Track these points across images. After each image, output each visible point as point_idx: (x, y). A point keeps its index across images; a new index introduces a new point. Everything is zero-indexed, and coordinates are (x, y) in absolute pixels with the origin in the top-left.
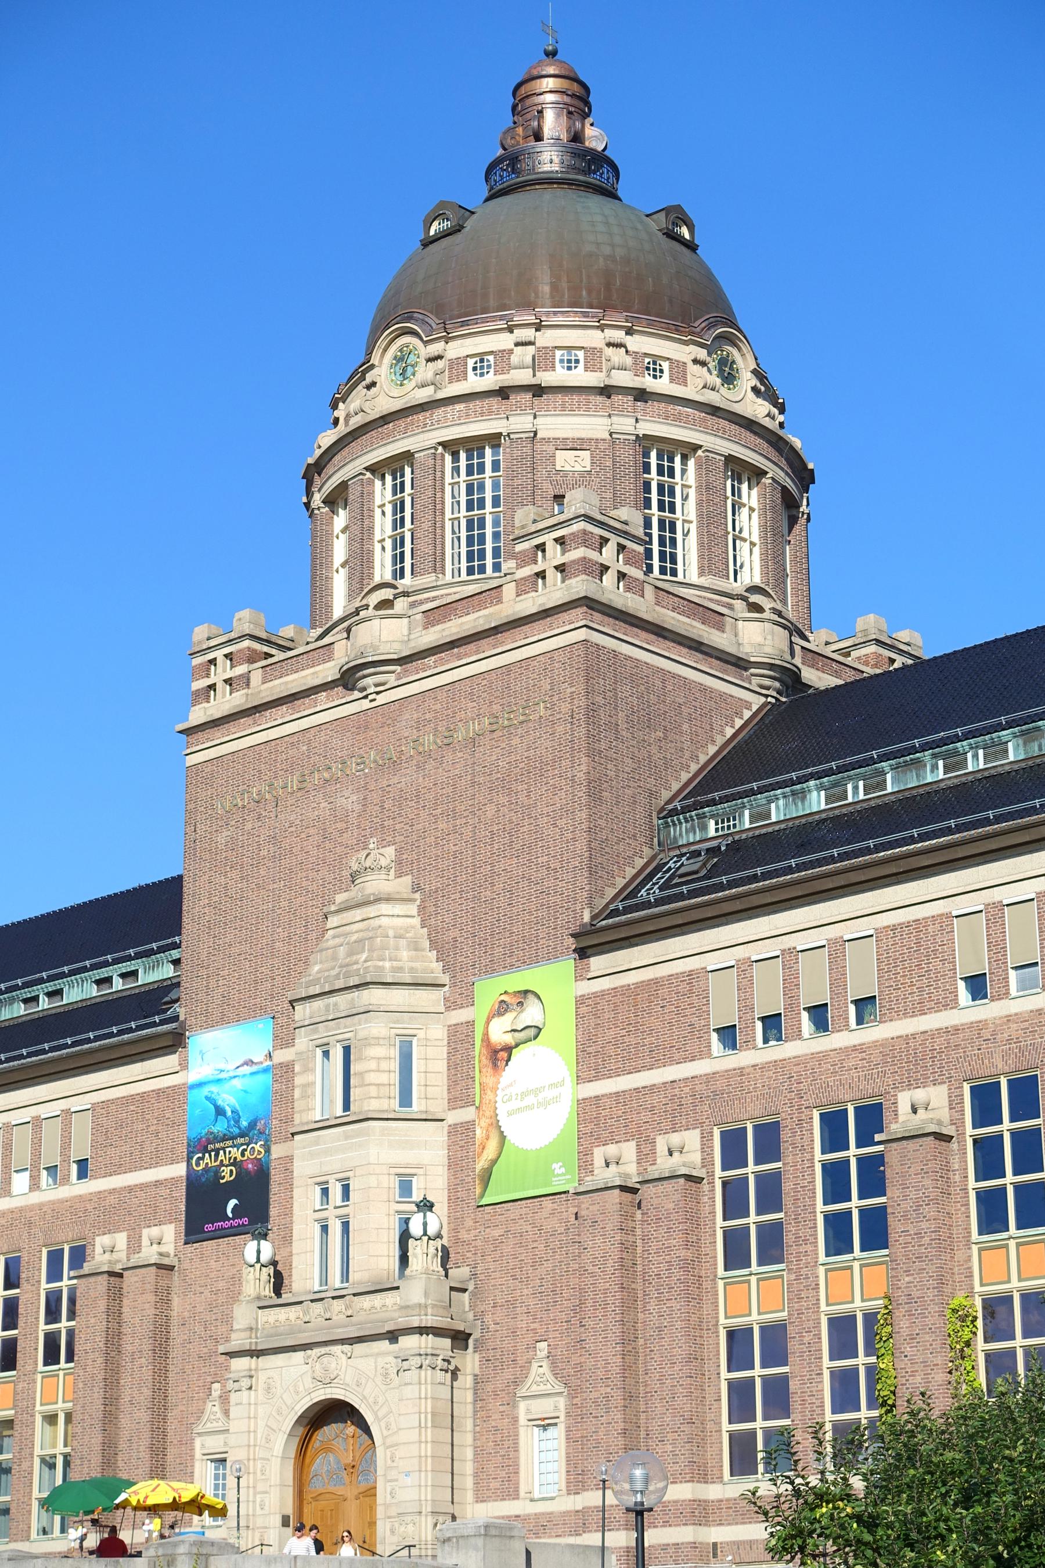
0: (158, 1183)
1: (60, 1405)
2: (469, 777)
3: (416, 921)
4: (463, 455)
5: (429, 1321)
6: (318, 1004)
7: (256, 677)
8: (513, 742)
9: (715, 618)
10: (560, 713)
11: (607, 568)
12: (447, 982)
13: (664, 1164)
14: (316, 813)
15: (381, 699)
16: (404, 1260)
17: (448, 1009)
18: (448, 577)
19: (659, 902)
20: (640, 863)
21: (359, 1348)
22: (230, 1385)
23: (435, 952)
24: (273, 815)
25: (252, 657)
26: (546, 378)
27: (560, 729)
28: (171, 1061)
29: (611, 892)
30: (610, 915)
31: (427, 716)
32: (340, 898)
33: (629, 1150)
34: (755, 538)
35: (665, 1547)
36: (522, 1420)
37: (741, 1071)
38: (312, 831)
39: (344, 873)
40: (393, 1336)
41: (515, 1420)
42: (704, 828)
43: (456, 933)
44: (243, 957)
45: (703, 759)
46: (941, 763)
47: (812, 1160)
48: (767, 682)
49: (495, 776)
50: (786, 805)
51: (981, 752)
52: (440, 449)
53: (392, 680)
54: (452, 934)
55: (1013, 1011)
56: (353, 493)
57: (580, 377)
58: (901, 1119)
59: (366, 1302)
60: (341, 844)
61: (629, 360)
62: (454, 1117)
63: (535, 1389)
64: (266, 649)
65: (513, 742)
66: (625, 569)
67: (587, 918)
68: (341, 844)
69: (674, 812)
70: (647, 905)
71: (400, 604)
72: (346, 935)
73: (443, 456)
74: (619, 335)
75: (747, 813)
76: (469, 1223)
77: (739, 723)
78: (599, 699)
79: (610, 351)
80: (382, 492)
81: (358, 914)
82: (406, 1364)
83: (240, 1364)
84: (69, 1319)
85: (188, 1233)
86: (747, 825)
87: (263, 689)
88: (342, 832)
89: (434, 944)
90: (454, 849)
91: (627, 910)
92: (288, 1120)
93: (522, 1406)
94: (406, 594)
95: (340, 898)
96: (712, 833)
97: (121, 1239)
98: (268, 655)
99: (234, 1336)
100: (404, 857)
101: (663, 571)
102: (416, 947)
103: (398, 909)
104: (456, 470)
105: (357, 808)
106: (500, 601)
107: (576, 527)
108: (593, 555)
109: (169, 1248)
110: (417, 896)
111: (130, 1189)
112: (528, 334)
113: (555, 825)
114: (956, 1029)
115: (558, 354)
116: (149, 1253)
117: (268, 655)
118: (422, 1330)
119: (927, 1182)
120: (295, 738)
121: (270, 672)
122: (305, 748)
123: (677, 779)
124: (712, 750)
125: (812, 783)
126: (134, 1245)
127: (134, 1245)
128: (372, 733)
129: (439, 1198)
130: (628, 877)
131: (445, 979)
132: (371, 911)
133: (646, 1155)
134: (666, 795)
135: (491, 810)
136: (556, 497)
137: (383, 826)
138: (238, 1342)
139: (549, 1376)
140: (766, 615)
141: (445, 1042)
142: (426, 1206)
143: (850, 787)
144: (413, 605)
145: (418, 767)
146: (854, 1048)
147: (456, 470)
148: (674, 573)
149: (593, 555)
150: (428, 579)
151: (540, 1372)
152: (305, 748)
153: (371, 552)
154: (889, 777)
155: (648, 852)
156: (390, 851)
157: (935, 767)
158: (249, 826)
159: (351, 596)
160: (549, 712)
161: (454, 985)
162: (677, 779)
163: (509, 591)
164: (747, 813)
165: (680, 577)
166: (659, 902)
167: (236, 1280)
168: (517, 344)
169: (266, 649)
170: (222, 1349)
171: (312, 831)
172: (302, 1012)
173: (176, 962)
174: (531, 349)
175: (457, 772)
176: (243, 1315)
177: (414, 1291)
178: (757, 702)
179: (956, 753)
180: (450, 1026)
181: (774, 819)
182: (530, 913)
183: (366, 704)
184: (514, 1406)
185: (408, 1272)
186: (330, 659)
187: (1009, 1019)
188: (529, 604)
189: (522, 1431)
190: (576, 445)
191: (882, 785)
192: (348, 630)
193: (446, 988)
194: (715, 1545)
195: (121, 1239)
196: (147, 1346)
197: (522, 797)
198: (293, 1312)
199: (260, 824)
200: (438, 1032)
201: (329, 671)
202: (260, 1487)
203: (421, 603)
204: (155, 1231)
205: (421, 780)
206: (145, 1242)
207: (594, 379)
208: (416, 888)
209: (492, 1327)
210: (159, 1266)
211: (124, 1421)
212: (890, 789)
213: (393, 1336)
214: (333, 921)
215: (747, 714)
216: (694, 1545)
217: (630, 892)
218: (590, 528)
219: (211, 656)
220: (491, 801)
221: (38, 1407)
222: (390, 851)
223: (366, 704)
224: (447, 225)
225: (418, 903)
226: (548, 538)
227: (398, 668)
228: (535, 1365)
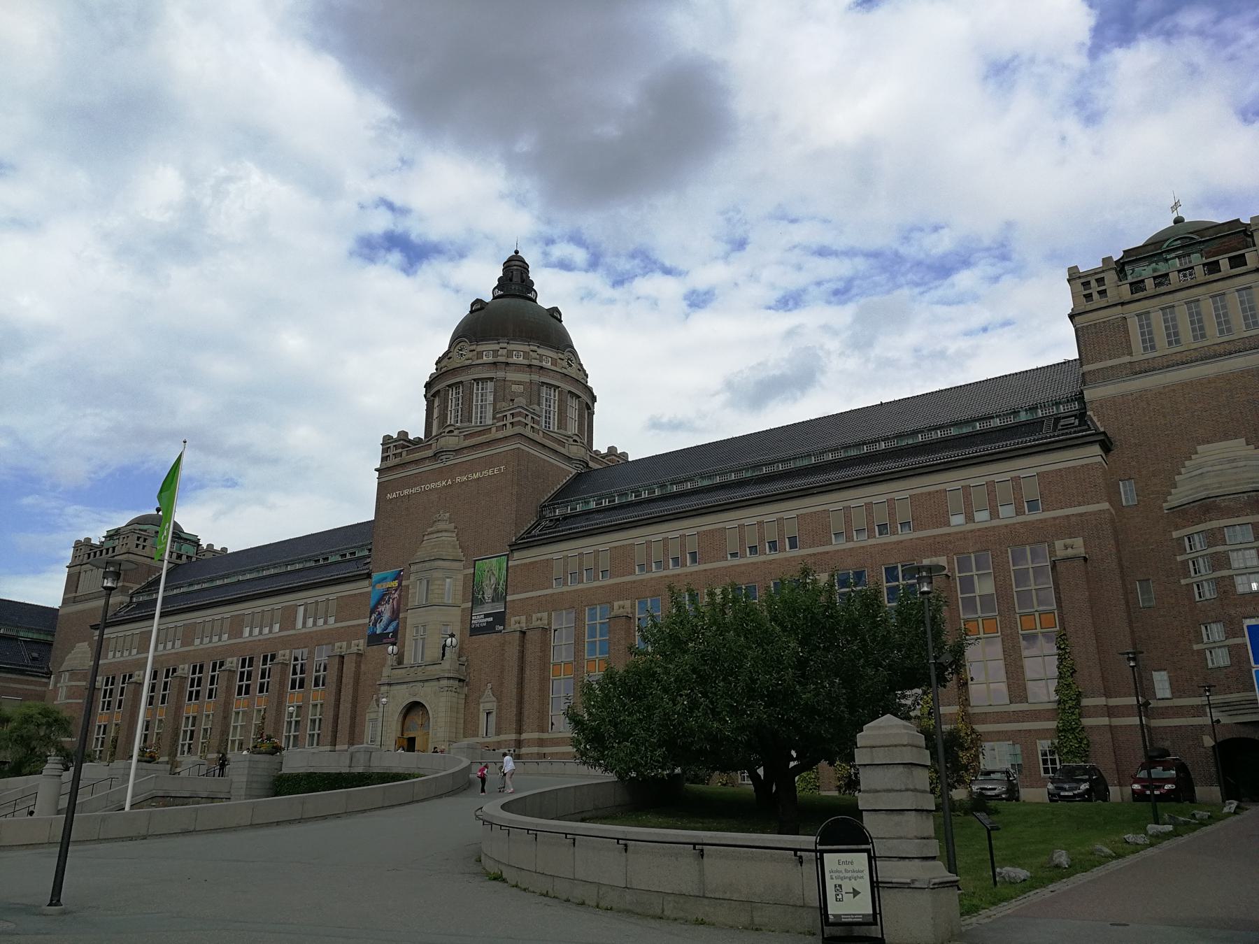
0: (359, 625)
1: (319, 701)
3: (455, 539)
4: (480, 383)
5: (451, 675)
6: (420, 565)
7: (404, 454)
9: (562, 444)
11: (527, 424)
13: (535, 624)
15: (448, 463)
16: (444, 655)
17: (464, 569)
18: (473, 424)
19: (539, 536)
20: (532, 523)
21: (426, 684)
22: (380, 695)
25: (403, 447)
26: (510, 360)
28: (366, 583)
29: (522, 532)
30: (524, 539)
32: (429, 530)
33: (523, 618)
34: (577, 419)
35: (528, 754)
36: (481, 710)
37: (562, 593)
40: (438, 679)
41: (479, 710)
42: (555, 512)
45: (556, 489)
46: (633, 495)
47: (584, 624)
48: (578, 466)
50: (582, 506)
51: (647, 492)
52: (473, 381)
53: (452, 457)
55: (653, 576)
56: (442, 394)
57: (521, 360)
58: (615, 611)
59: (429, 668)
61: (538, 357)
62: (464, 606)
63: (486, 700)
64: (408, 444)
66: (533, 425)
67: (514, 540)
69: (545, 506)
70: (534, 536)
71: (456, 432)
72: (432, 542)
73: (473, 384)
74: (535, 348)
75: (569, 508)
76: (467, 642)
77: (568, 478)
78: (522, 468)
79: (531, 353)
80: (452, 394)
81: (435, 536)
82: (442, 690)
83: (384, 689)
84: (324, 671)
85: (368, 643)
86: (569, 512)
87: (406, 457)
89: (461, 547)
91: (527, 538)
92: (407, 605)
93: (481, 705)
94: (458, 429)
95: (429, 530)
96: (557, 514)
97: (345, 644)
98: (409, 447)
99: (382, 679)
101: (546, 426)
102: (454, 546)
103: (449, 534)
104: (478, 389)
106: (490, 433)
107: (517, 410)
108: (523, 420)
109: (362, 648)
110: (456, 530)
111: (348, 627)
112: (505, 345)
114: (634, 582)
115: (514, 352)
116: (354, 649)
117: (409, 447)
118: (449, 678)
119: (623, 632)
120: (416, 475)
121: (408, 453)
123: (547, 495)
124: (559, 487)
125: (591, 499)
126: (349, 646)
127: (349, 646)
129: (457, 633)
130: (529, 527)
131: (464, 559)
132: (440, 535)
133: (529, 620)
134: (543, 500)
136: (511, 400)
138: (384, 680)
139: (491, 695)
140: (579, 444)
142: (452, 636)
143: (604, 501)
144: (460, 433)
146: (601, 587)
147: (478, 389)
148: (549, 428)
149: (523, 420)
150: (466, 424)
151: (488, 692)
153: (447, 414)
154: (616, 498)
155: (535, 519)
157: (632, 496)
158: (398, 504)
159: (439, 428)
161: (466, 561)
162: (547, 495)
163: (494, 430)
164: (569, 508)
165: (551, 429)
166: (539, 536)
167: (385, 659)
168: (501, 348)
169: (408, 444)
170: (378, 683)
172: (413, 568)
173: (370, 550)
174: (506, 350)
176: (386, 671)
177: (446, 664)
178: (574, 472)
179: (638, 491)
181: (578, 510)
183: (442, 465)
184: (479, 704)
185: (445, 658)
186: (431, 449)
187: (652, 579)
188: (500, 435)
189: (481, 714)
190: (519, 383)
191: (614, 501)
192: (437, 440)
194: (544, 754)
195: (345, 644)
196: (351, 681)
198: (404, 671)
200: (460, 577)
201: (430, 453)
202: (389, 731)
203: (463, 432)
204: (356, 642)
206: (352, 645)
207: (526, 362)
208: (456, 528)
209: (473, 678)
210: (357, 654)
211: (342, 707)
212: (616, 502)
213: (438, 679)
214: (426, 538)
215: (571, 476)
216: (538, 754)
217: (529, 532)
218: (522, 411)
219: (389, 445)
221: (311, 702)
223: (442, 465)
224: (479, 307)
226: (508, 413)
227: (454, 454)
228: (486, 691)
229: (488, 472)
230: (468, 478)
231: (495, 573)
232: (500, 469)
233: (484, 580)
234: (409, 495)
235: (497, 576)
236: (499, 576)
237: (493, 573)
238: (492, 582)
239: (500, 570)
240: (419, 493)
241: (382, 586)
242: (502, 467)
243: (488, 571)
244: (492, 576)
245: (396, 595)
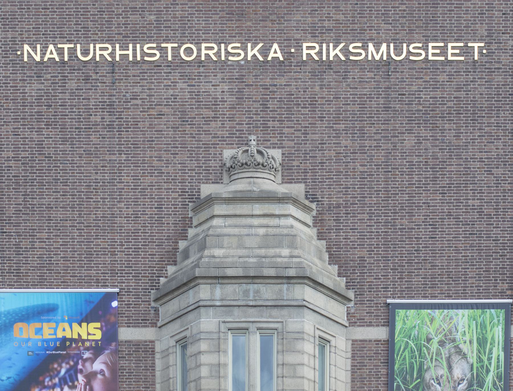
2: (382, 101)
8: (440, 78)
10: (499, 62)
12: (353, 298)
14: (171, 92)
17: (352, 324)
23: (336, 267)
24: (108, 80)
27: (498, 79)
31: (326, 24)
38: (165, 110)
39: (212, 163)
43: (365, 253)
44: (69, 223)
49: (414, 107)
54: (358, 253)
60: (207, 132)
65: (440, 78)
68: (207, 132)
88: (207, 121)
90: (361, 169)
100: (295, 163)
105: (231, 99)
113: (490, 172)
122: (153, 17)
128: (249, 24)
131: (351, 294)
135: (409, 141)
137: (266, 127)
141: (349, 355)
145: (313, 73)
152: (153, 17)
156: (277, 154)
158: (72, 85)
160: (485, 59)
171: (165, 110)
175: (365, 91)
180: (356, 341)
182: (457, 251)
193: (352, 304)
197: (450, 136)
199: (89, 86)
205: (317, 88)
208: (311, 197)
220: (410, 131)
222: (277, 154)
225: (314, 213)
229: (426, 50)
230: (346, 51)
231: (465, 348)
232: (466, 51)
233: (427, 363)
234: (113, 64)
235: (473, 359)
236: (480, 360)
237: (459, 351)
238: (457, 373)
239: (482, 342)
240: (156, 65)
241: (39, 331)
242: (476, 45)
243: (442, 343)
244: (456, 359)
245: (98, 366)
